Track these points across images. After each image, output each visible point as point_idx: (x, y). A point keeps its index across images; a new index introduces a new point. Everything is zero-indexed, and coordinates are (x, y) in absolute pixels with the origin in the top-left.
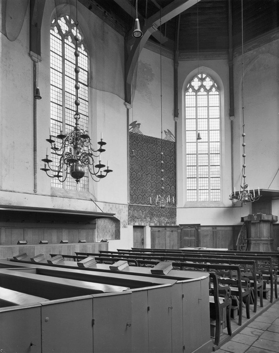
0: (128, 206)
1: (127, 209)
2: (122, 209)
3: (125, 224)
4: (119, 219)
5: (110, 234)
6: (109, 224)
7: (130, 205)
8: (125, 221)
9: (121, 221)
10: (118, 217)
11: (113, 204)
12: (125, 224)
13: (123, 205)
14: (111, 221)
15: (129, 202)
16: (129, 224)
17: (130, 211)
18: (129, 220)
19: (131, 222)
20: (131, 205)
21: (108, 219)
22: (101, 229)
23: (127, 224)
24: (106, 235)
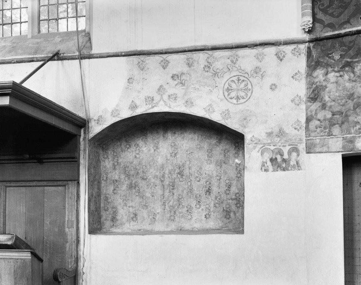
0: (303, 47)
1: (302, 63)
2: (257, 70)
3: (286, 151)
4: (240, 131)
5: (211, 201)
6: (202, 155)
7: (316, 41)
8: (281, 133)
9: (248, 138)
10: (226, 114)
11: (189, 54)
12: (286, 151)
13: (272, 50)
14: (214, 141)
15: (310, 19)
16: (309, 150)
17: (319, 73)
18: (314, 123)
19: (330, 134)
20: (330, 33)
21: (196, 136)
22: (158, 182)
23: (295, 149)
24: (189, 210)
